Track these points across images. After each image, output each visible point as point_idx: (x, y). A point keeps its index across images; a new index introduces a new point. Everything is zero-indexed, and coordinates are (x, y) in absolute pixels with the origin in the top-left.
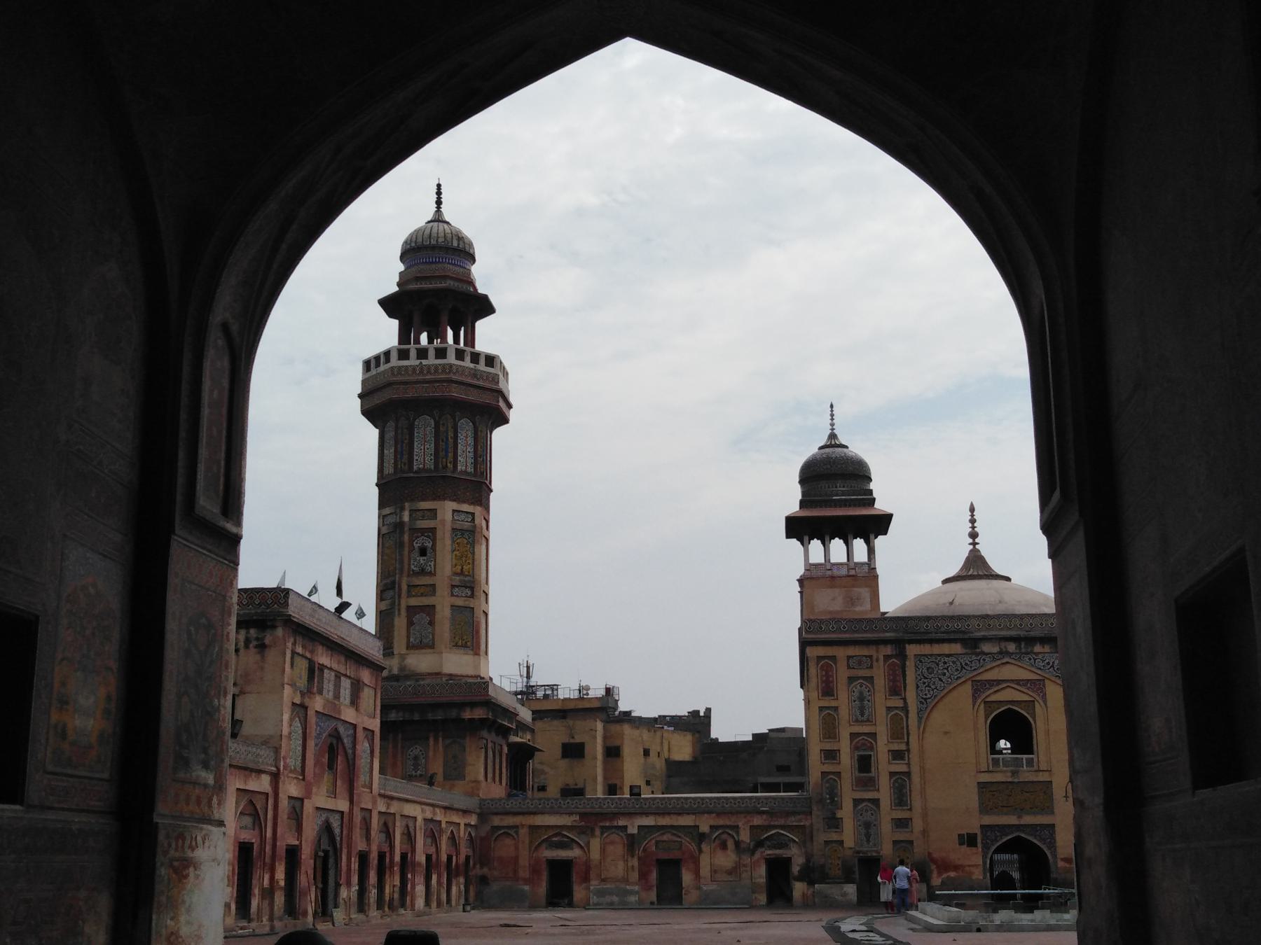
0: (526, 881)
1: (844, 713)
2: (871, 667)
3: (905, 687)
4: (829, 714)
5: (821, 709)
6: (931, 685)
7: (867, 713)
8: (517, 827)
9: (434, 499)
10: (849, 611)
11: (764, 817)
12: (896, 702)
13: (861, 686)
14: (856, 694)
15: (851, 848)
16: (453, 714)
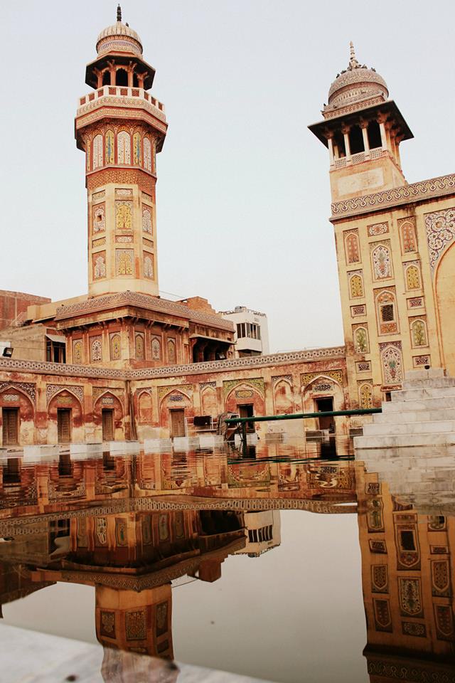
0: (157, 425)
1: (367, 275)
2: (388, 231)
3: (417, 242)
4: (356, 276)
5: (349, 272)
6: (440, 237)
7: (387, 271)
8: (150, 388)
9: (104, 184)
10: (366, 190)
11: (310, 365)
12: (412, 256)
13: (381, 249)
14: (378, 256)
15: (380, 385)
16: (110, 316)
